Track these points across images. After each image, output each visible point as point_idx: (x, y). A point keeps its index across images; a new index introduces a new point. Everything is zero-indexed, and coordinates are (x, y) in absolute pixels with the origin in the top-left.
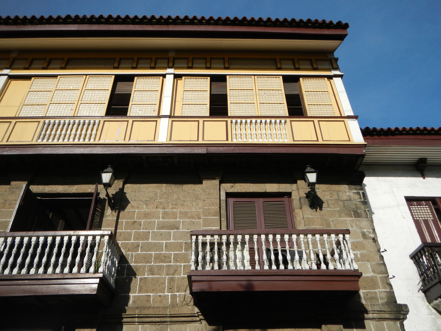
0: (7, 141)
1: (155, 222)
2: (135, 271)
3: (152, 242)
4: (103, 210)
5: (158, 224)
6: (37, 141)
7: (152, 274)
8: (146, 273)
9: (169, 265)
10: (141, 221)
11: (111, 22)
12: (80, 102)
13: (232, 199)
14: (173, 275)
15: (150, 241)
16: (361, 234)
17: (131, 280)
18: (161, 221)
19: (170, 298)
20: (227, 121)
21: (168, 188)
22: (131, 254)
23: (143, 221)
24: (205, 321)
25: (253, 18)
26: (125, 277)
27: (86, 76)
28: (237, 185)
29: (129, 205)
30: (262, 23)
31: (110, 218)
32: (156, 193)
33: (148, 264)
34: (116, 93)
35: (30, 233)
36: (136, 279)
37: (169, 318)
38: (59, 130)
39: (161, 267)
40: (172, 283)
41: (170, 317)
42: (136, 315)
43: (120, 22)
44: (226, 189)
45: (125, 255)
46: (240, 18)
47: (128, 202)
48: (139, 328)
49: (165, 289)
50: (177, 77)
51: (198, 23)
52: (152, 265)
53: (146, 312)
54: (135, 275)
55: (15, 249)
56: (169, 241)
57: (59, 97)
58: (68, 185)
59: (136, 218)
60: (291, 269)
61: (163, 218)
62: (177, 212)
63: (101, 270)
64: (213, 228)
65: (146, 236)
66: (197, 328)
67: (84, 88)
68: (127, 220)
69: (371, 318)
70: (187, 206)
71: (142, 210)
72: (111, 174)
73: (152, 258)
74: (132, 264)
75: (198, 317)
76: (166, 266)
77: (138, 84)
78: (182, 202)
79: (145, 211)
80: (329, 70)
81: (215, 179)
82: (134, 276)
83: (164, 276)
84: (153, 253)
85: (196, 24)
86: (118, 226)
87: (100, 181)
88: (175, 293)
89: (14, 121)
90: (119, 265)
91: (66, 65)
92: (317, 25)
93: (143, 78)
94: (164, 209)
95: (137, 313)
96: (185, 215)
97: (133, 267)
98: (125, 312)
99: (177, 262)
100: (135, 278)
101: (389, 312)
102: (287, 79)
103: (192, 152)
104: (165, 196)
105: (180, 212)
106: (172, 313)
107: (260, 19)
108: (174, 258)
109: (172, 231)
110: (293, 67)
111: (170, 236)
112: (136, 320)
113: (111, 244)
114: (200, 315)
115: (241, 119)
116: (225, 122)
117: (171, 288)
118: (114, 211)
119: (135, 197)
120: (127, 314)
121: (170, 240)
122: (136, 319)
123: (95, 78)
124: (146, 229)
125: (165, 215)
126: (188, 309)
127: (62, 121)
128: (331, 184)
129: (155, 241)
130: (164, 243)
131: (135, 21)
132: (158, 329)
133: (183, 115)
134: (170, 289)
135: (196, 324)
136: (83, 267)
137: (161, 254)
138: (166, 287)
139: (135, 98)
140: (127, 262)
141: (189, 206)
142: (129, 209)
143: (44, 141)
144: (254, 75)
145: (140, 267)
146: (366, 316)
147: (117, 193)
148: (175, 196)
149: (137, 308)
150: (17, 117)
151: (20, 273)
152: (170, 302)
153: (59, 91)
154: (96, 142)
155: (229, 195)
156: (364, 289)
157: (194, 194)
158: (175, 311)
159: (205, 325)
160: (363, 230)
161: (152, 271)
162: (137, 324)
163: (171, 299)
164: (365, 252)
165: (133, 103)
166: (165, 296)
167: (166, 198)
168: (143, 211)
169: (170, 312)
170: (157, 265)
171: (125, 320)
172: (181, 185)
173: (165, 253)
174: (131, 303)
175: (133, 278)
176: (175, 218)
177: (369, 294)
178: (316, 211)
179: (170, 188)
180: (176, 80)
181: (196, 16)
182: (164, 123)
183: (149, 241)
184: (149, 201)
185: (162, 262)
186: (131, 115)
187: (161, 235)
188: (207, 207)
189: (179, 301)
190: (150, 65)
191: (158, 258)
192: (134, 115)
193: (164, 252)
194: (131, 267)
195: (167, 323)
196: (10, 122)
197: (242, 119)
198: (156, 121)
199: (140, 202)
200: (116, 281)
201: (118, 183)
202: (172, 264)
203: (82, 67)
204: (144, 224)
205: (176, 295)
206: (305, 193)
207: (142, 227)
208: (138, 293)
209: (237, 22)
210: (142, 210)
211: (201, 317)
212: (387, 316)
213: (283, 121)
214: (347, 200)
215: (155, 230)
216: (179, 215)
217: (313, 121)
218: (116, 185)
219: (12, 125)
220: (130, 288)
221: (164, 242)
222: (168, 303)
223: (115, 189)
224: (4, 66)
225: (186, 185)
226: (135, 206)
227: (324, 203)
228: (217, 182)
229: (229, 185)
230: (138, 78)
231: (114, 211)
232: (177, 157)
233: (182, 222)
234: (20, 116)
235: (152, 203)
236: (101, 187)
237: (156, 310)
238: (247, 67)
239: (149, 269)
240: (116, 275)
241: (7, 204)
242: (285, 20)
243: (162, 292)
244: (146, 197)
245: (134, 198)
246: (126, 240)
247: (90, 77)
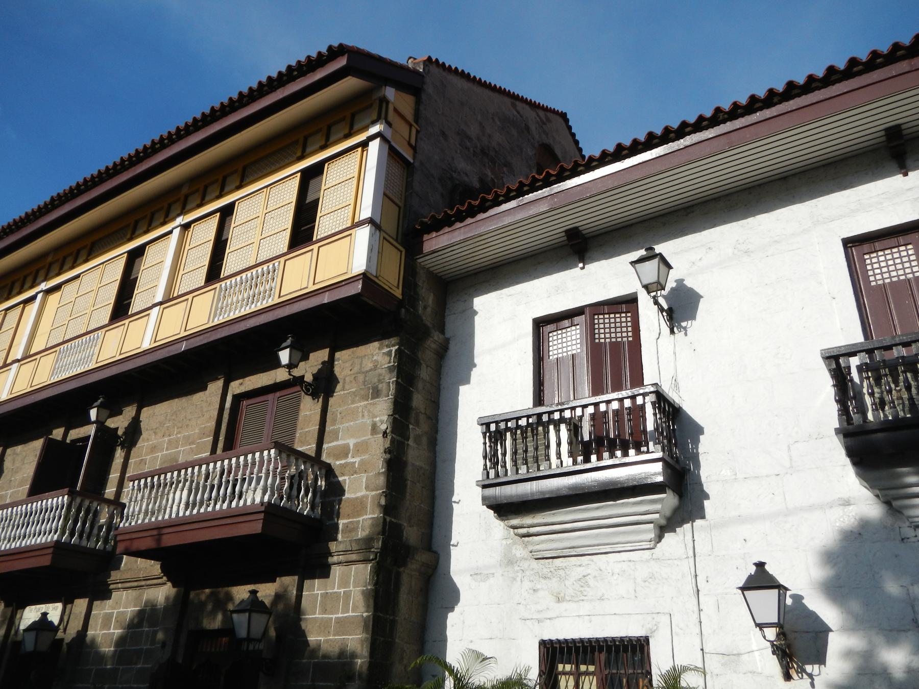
16: (370, 428)
41: (144, 580)
42: (117, 580)
50: (186, 227)
69: (336, 562)
79: (153, 444)
92: (305, 68)
93: (353, 153)
95: (118, 578)
101: (356, 552)
122: (120, 584)
128: (358, 346)
156: (346, 519)
160: (375, 420)
162: (122, 590)
164: (366, 457)
169: (143, 574)
171: (112, 587)
177: (349, 526)
212: (354, 557)
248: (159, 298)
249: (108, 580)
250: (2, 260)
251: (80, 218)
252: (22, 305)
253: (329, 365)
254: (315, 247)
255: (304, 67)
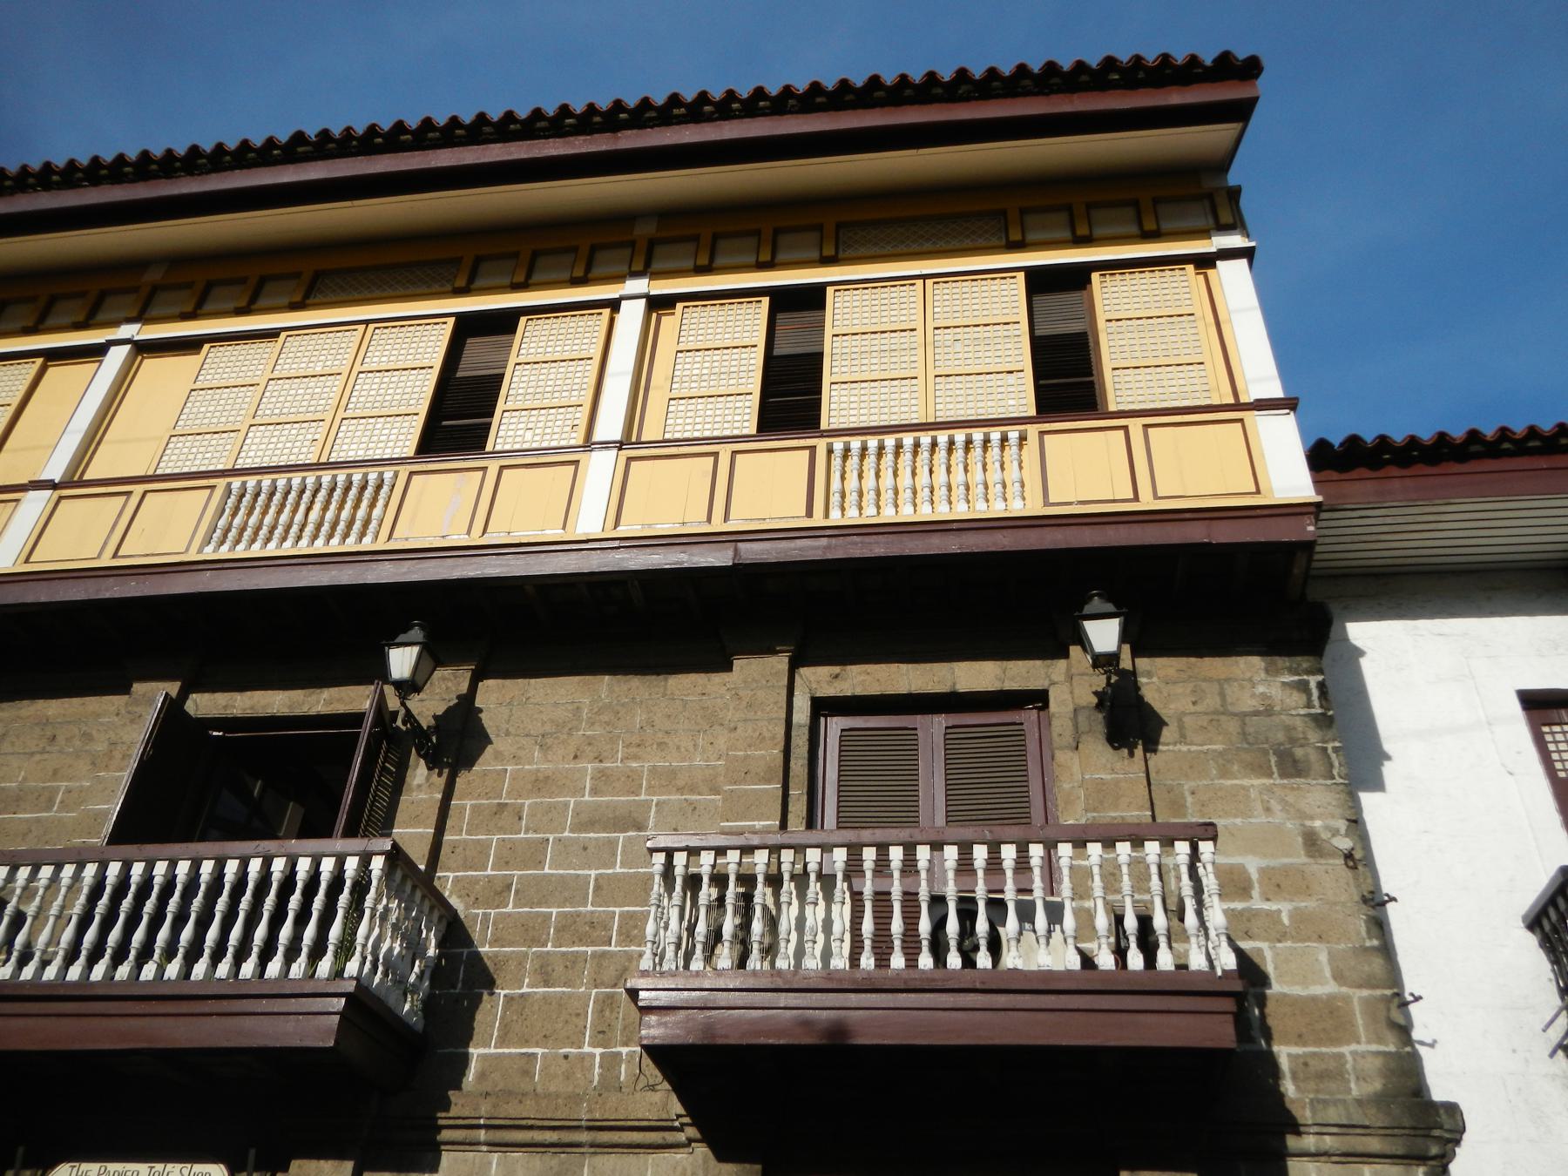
0: (115, 556)
1: (566, 805)
2: (492, 971)
3: (552, 875)
4: (403, 768)
5: (577, 814)
6: (200, 551)
7: (547, 984)
8: (527, 980)
9: (604, 954)
10: (523, 804)
11: (431, 140)
12: (342, 413)
13: (835, 719)
14: (615, 986)
15: (547, 870)
16: (1300, 839)
17: (476, 1002)
18: (586, 802)
19: (597, 1065)
20: (813, 449)
21: (616, 689)
22: (484, 914)
23: (527, 802)
24: (704, 1145)
25: (903, 77)
26: (457, 991)
27: (364, 326)
28: (854, 670)
29: (489, 749)
30: (939, 91)
31: (423, 796)
32: (578, 708)
33: (534, 949)
34: (459, 374)
35: (151, 849)
36: (494, 997)
37: (586, 1133)
38: (317, 507)
39: (574, 961)
40: (607, 1013)
41: (590, 1128)
42: (480, 1118)
43: (460, 137)
44: (814, 686)
45: (462, 917)
46: (859, 81)
47: (483, 740)
48: (490, 1163)
49: (585, 1034)
51: (716, 115)
52: (548, 952)
53: (512, 1110)
54: (490, 983)
55: (105, 900)
56: (610, 871)
57: (282, 401)
58: (302, 688)
59: (508, 793)
60: (985, 969)
61: (595, 791)
62: (643, 772)
63: (352, 967)
64: (756, 823)
65: (534, 854)
66: (679, 1169)
67: (357, 368)
68: (477, 799)
69: (1313, 1149)
70: (678, 748)
71: (527, 767)
72: (416, 649)
73: (550, 928)
74: (484, 949)
75: (680, 1129)
76: (594, 954)
77: (532, 339)
78: (660, 735)
79: (538, 770)
80: (1205, 234)
81: (773, 652)
82: (486, 988)
83: (583, 989)
84: (554, 911)
85: (709, 119)
86: (449, 823)
87: (379, 671)
88: (615, 1047)
89: (138, 489)
90: (445, 951)
91: (307, 295)
92: (1141, 75)
94: (601, 761)
95: (483, 1113)
96: (666, 779)
97: (486, 960)
98: (447, 1109)
99: (631, 941)
100: (492, 994)
101: (1382, 1132)
102: (1040, 282)
103: (683, 562)
104: (605, 718)
105: (653, 770)
106: (598, 1116)
107: (931, 76)
108: (620, 927)
109: (622, 835)
110: (1134, 230)
111: (614, 855)
112: (482, 1135)
113: (395, 884)
114: (687, 1125)
115: (863, 438)
116: (807, 452)
117: (603, 1032)
118: (437, 771)
119: (508, 722)
120: (450, 1115)
121: (613, 865)
122: (483, 1132)
123: (394, 330)
124: (535, 831)
125: (603, 781)
126: (651, 1104)
127: (357, 477)
128: (1200, 655)
129: (561, 872)
130: (593, 876)
131: (509, 128)
132: (551, 1168)
133: (668, 436)
134: (599, 1032)
135: (679, 1156)
136: (299, 960)
137: (579, 914)
138: (588, 1026)
139: (517, 388)
140: (467, 941)
141: (683, 750)
142: (486, 763)
143: (348, 541)
144: (924, 277)
145: (508, 957)
146: (1292, 1142)
147: (449, 711)
148: (639, 717)
149: (487, 1094)
150: (150, 476)
151: (113, 978)
152: (596, 1078)
153: (279, 382)
154: (381, 545)
155: (823, 707)
156: (1296, 1044)
157: (703, 708)
158: (612, 1108)
159: (705, 1161)
160: (1308, 823)
161: (547, 973)
162: (485, 1148)
163: (601, 1066)
164: (1309, 904)
165: (510, 405)
166: (582, 1057)
167: (608, 723)
168: (530, 771)
169: (590, 1111)
170: (564, 954)
171: (445, 1135)
172: (661, 677)
173: (592, 912)
174: (470, 1079)
175: (486, 997)
176: (633, 793)
177: (1312, 1062)
178: (1131, 754)
179: (625, 688)
180: (654, 315)
181: (708, 90)
182: (601, 467)
183: (543, 869)
184: (551, 734)
185: (581, 940)
186: (498, 448)
187: (585, 849)
188: (741, 750)
189: (626, 1076)
190: (630, 267)
191: (572, 929)
192: (507, 447)
193: (590, 908)
194: (481, 959)
195: (582, 1150)
196: (129, 493)
197: (868, 437)
198: (576, 462)
199: (524, 741)
200: (429, 1006)
201: (456, 677)
202: (612, 948)
203: (392, 293)
204: (532, 815)
205: (620, 1054)
206: (1094, 690)
207: (524, 822)
208: (496, 1047)
209: (849, 97)
210: (527, 767)
211: (692, 1132)
212: (1374, 1144)
213: (1013, 435)
214: (1256, 713)
215: (566, 834)
216: (649, 781)
217: (1125, 428)
218: (450, 684)
219: (134, 500)
220: (473, 1029)
221: (593, 873)
222: (592, 1082)
223: (444, 700)
224: (123, 315)
225: (680, 676)
226: (506, 753)
227: (1167, 724)
228: (780, 663)
229: (824, 672)
230: (532, 319)
231: (437, 771)
232: (636, 583)
233: (657, 805)
234: (159, 472)
235: (564, 742)
236: (389, 690)
237: (544, 1103)
238: (902, 249)
239: (536, 967)
240: (427, 984)
241: (117, 755)
242: (1022, 69)
243: (572, 1045)
244: (544, 723)
245: (504, 726)
246: (471, 868)
247: (379, 328)
248: (55, 472)
249: (439, 1115)
250: (4, 240)
251: (356, 203)
252: (39, 361)
253: (466, 704)
254: (493, 466)
255: (1141, 73)
